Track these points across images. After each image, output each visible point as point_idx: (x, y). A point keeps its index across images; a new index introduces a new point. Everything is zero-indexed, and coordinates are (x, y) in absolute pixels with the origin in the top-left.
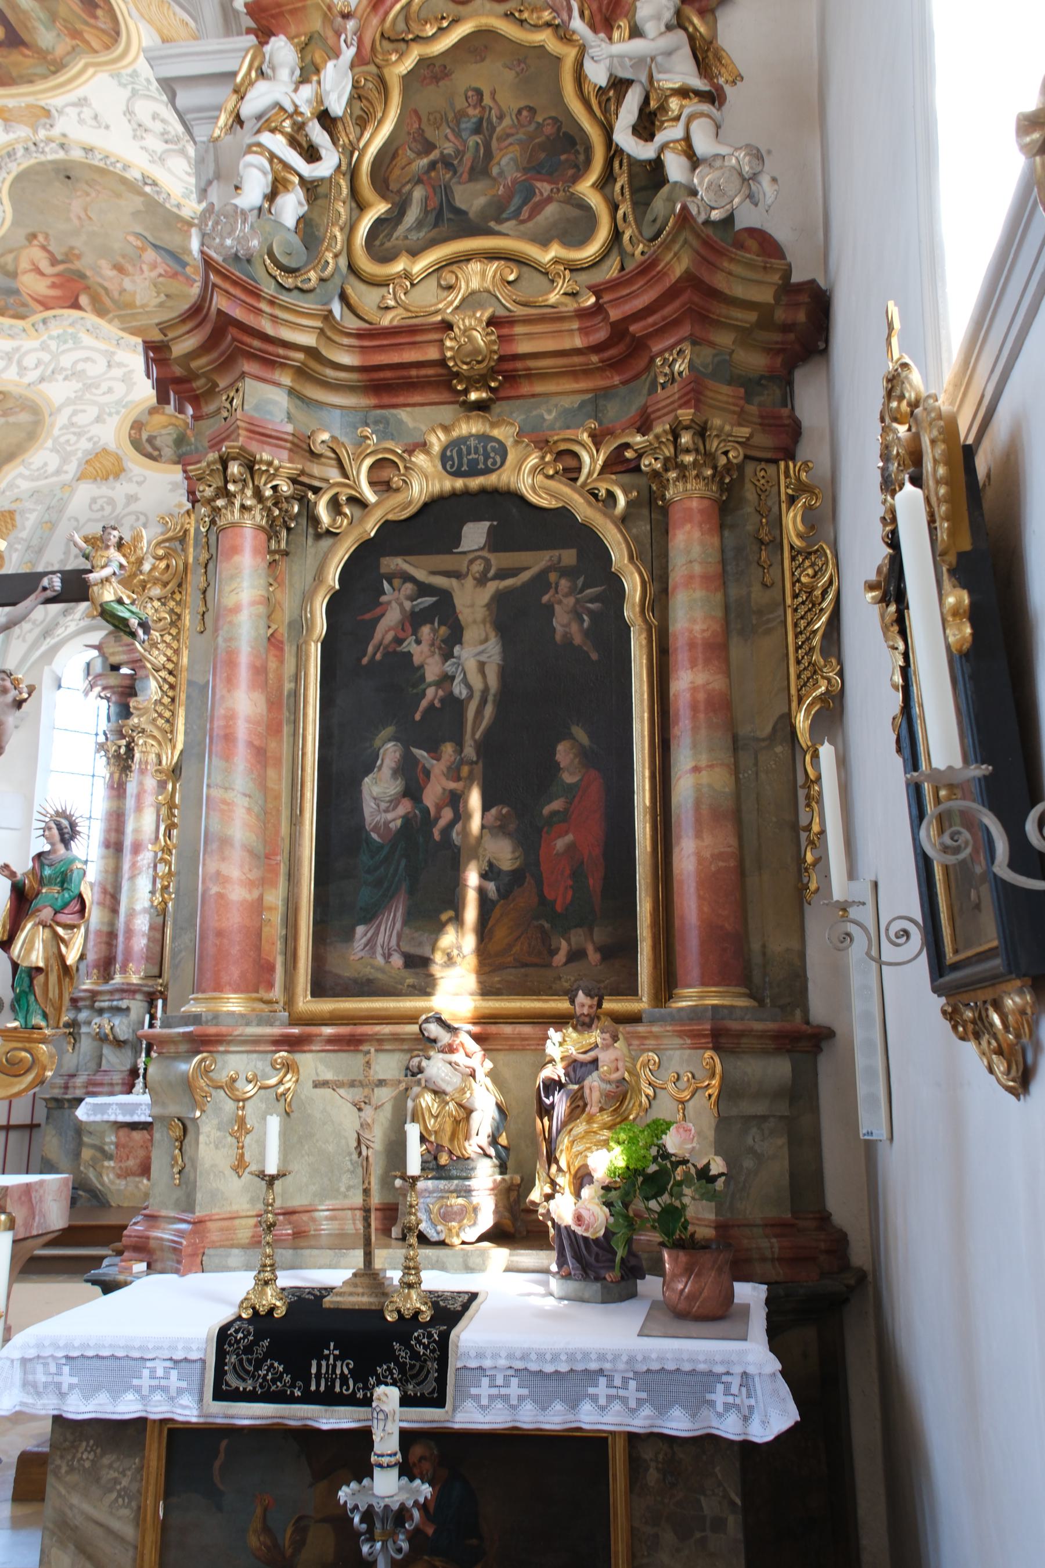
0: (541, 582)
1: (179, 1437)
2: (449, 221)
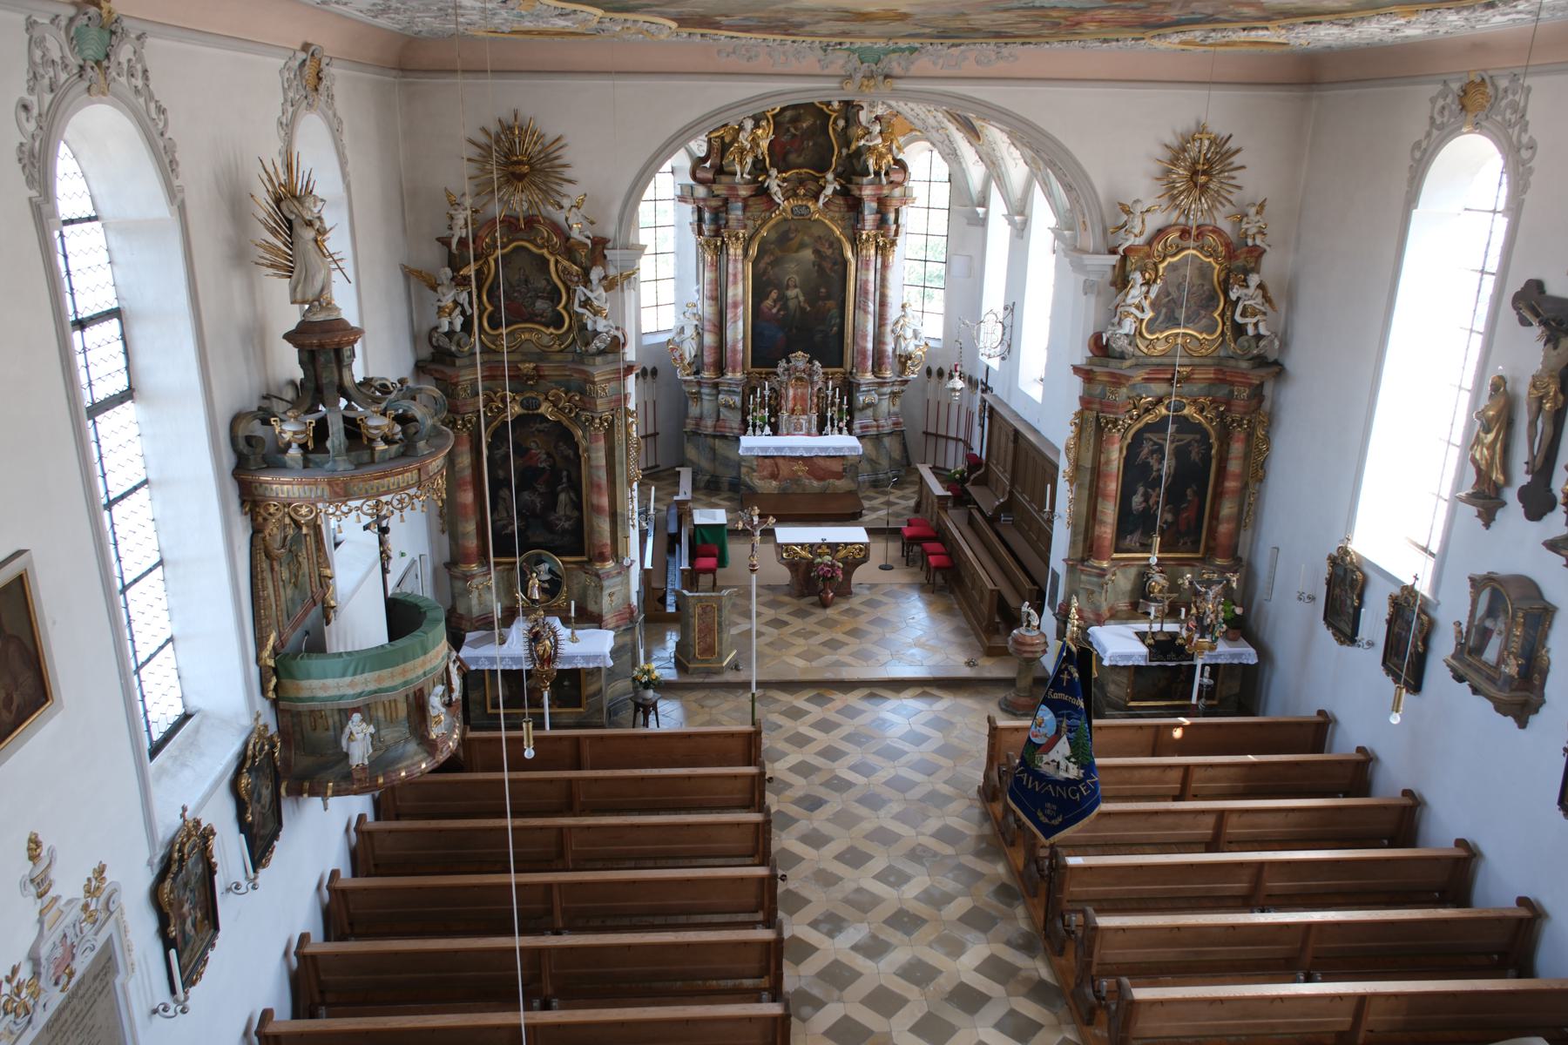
1: (1138, 668)
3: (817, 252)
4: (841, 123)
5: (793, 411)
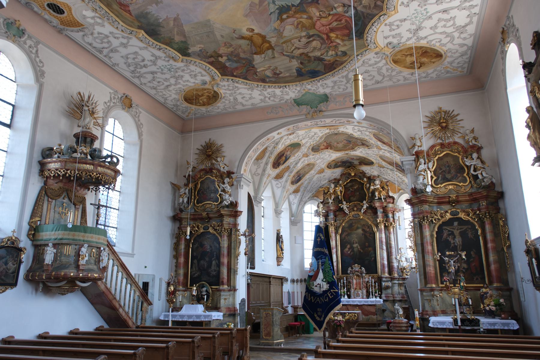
0: (466, 230)
2: (445, 180)
3: (363, 230)
4: (368, 185)
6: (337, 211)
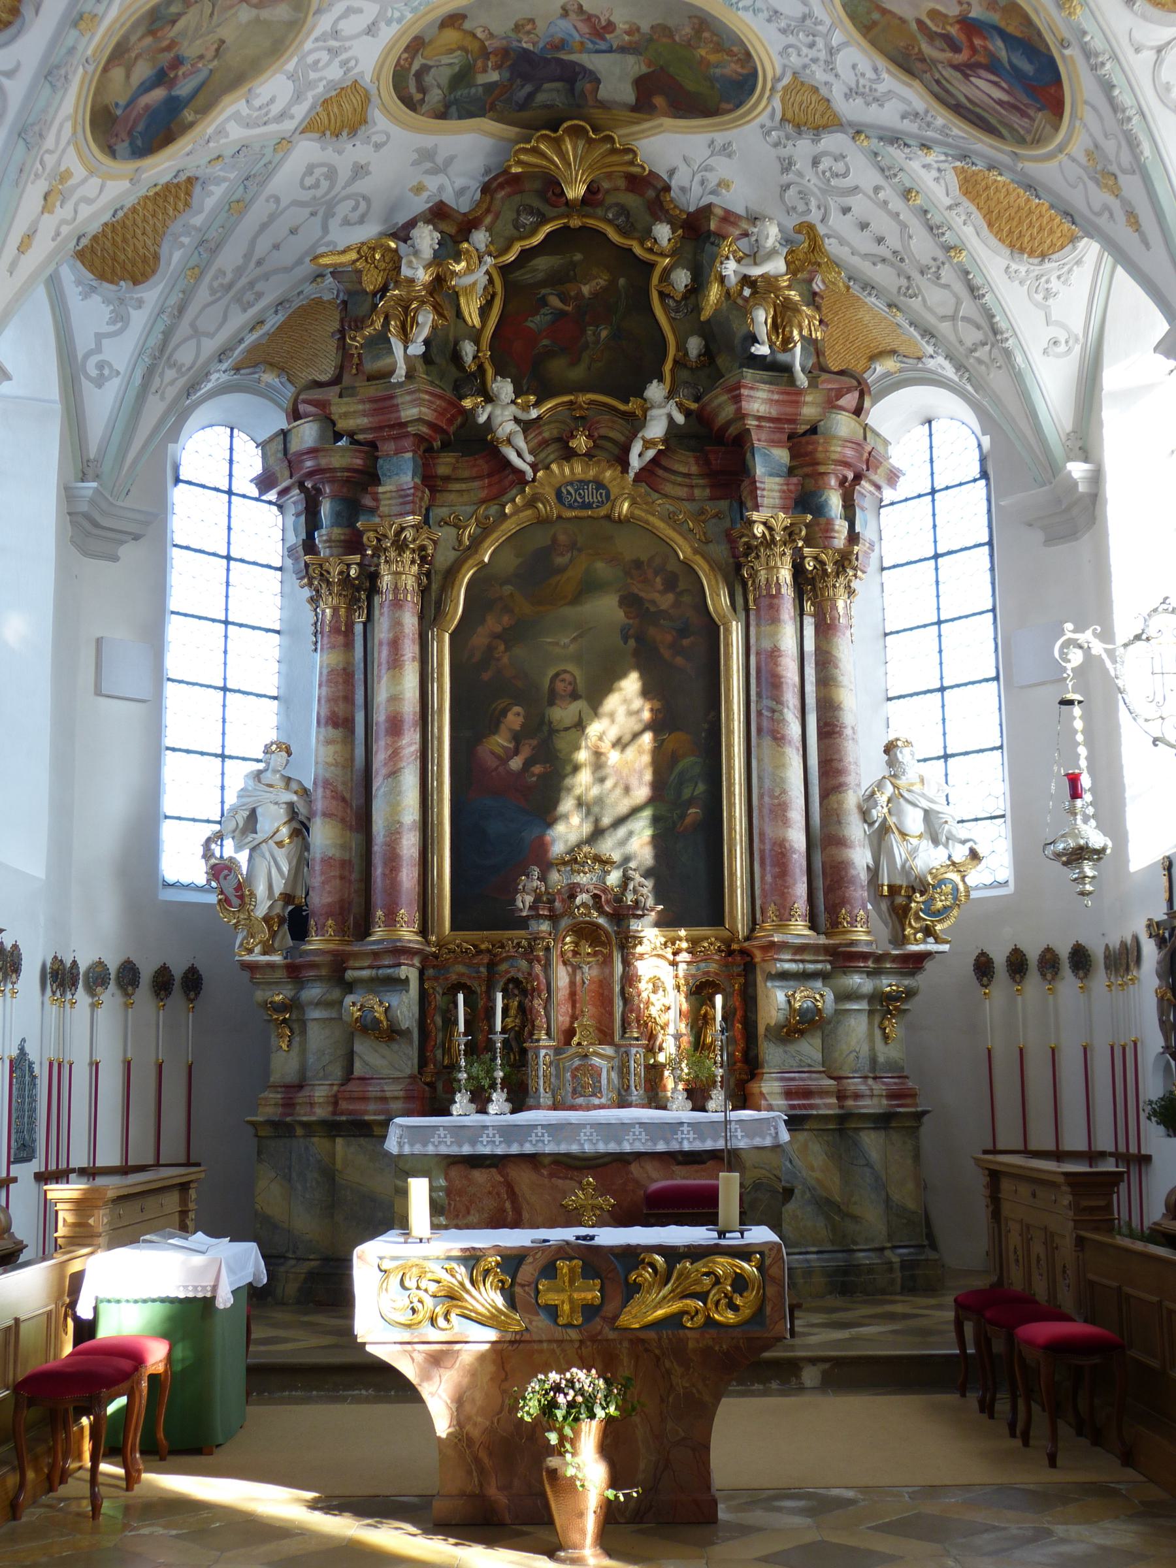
3: (630, 602)
4: (682, 278)
5: (570, 1033)
6: (446, 446)
